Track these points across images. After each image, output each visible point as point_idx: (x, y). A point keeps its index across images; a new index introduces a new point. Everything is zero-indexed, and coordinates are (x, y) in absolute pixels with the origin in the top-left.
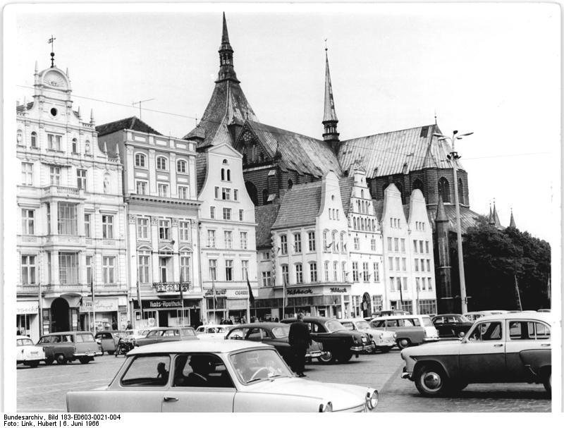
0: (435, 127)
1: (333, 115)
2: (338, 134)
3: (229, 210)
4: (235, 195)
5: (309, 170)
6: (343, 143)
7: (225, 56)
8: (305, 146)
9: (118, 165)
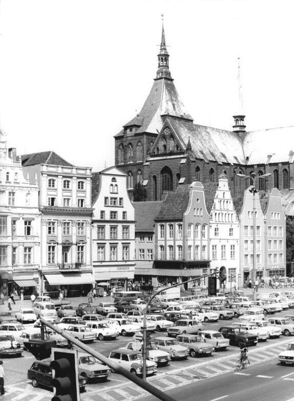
3: (115, 212)
4: (120, 202)
6: (249, 133)
7: (162, 59)
9: (36, 188)
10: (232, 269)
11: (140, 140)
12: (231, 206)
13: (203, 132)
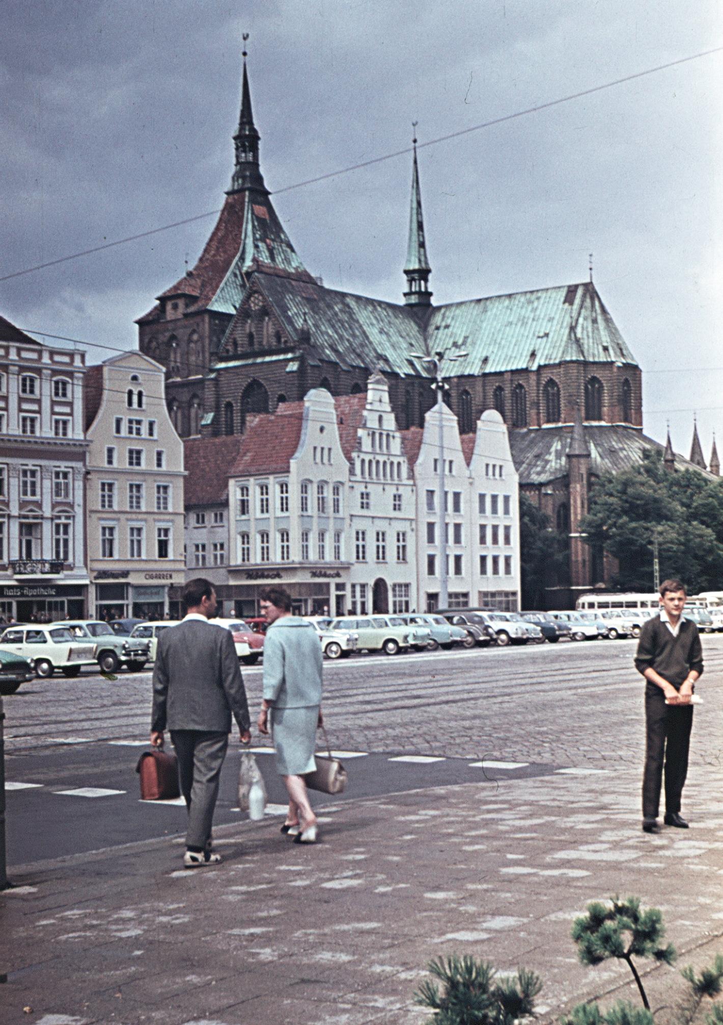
0: (589, 289)
1: (423, 259)
2: (431, 294)
3: (139, 452)
5: (363, 362)
6: (439, 308)
7: (243, 146)
8: (363, 316)
10: (400, 585)
11: (195, 327)
12: (396, 446)
13: (336, 304)
